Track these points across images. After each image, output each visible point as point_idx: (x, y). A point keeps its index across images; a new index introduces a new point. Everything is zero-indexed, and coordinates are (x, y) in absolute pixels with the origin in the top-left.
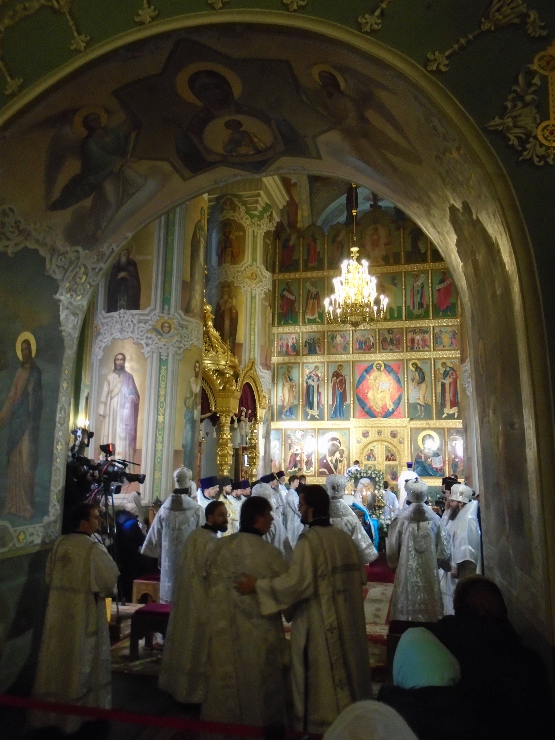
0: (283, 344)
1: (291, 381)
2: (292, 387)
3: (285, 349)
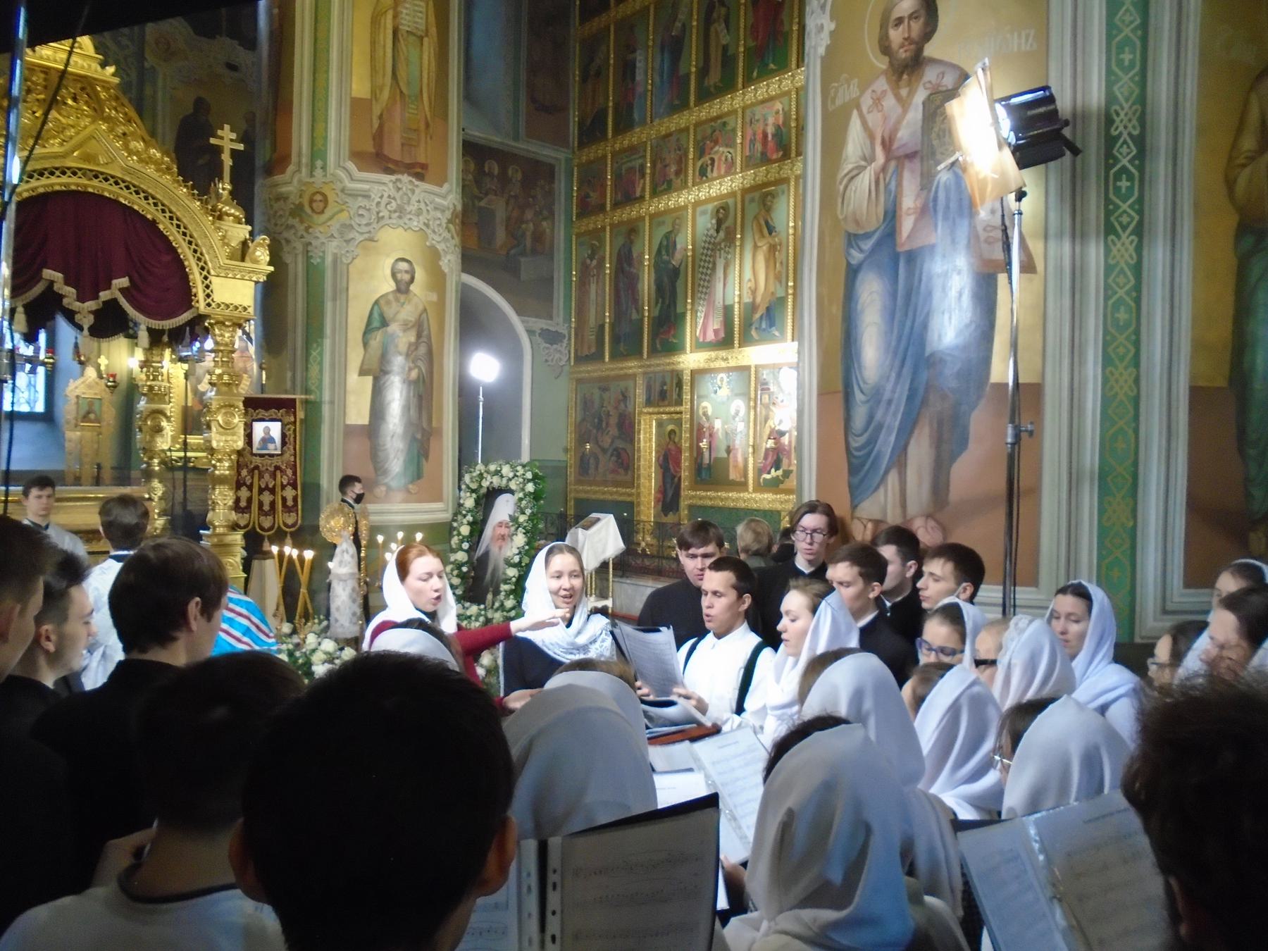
0: (754, 135)
1: (770, 233)
2: (773, 249)
3: (759, 146)
